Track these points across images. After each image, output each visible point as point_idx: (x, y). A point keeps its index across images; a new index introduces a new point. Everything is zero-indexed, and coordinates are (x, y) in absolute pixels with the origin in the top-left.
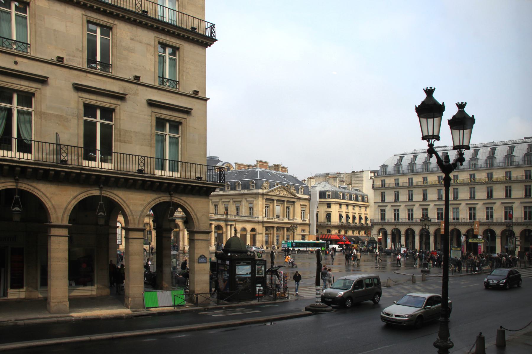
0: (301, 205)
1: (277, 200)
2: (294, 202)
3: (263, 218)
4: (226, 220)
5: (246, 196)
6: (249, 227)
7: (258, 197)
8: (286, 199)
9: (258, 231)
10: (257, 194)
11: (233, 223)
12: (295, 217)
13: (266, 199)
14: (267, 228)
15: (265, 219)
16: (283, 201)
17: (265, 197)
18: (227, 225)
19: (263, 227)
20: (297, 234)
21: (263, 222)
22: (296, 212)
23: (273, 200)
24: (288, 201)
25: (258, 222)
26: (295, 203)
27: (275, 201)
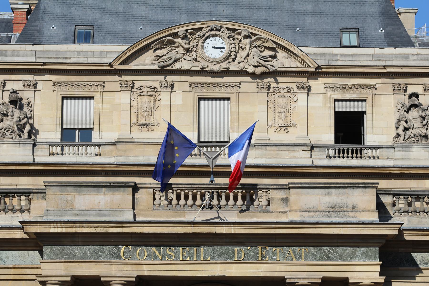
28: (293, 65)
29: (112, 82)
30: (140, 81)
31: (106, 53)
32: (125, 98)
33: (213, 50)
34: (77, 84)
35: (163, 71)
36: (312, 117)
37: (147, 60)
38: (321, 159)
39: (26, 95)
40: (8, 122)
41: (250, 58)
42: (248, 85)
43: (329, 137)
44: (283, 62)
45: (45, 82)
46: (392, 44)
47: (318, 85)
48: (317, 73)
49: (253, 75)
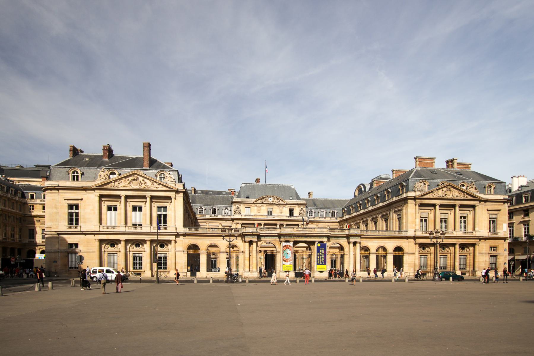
0: (488, 210)
1: (441, 206)
2: (474, 207)
3: (415, 231)
4: (348, 237)
5: (394, 205)
6: (390, 245)
7: (407, 203)
8: (458, 203)
9: (406, 250)
10: (406, 199)
11: (358, 240)
12: (476, 229)
13: (421, 205)
14: (423, 246)
15: (419, 234)
16: (454, 206)
17: (419, 201)
18: (349, 243)
19: (415, 244)
20: (481, 254)
21: (415, 238)
22: (477, 221)
23: (434, 206)
24: (461, 206)
25: (407, 238)
26: (477, 208)
27: (437, 207)
28: (283, 203)
29: (253, 205)
30: (258, 205)
31: (253, 200)
32: (256, 207)
33: (270, 200)
34: (248, 205)
35: (262, 203)
36: (286, 211)
37: (259, 202)
38: (287, 218)
39: (239, 207)
40: (237, 211)
41: (276, 201)
42: (275, 206)
43: (288, 215)
44: (281, 202)
45: (242, 205)
46: (298, 200)
47: (287, 206)
48: (287, 204)
49: (276, 204)
